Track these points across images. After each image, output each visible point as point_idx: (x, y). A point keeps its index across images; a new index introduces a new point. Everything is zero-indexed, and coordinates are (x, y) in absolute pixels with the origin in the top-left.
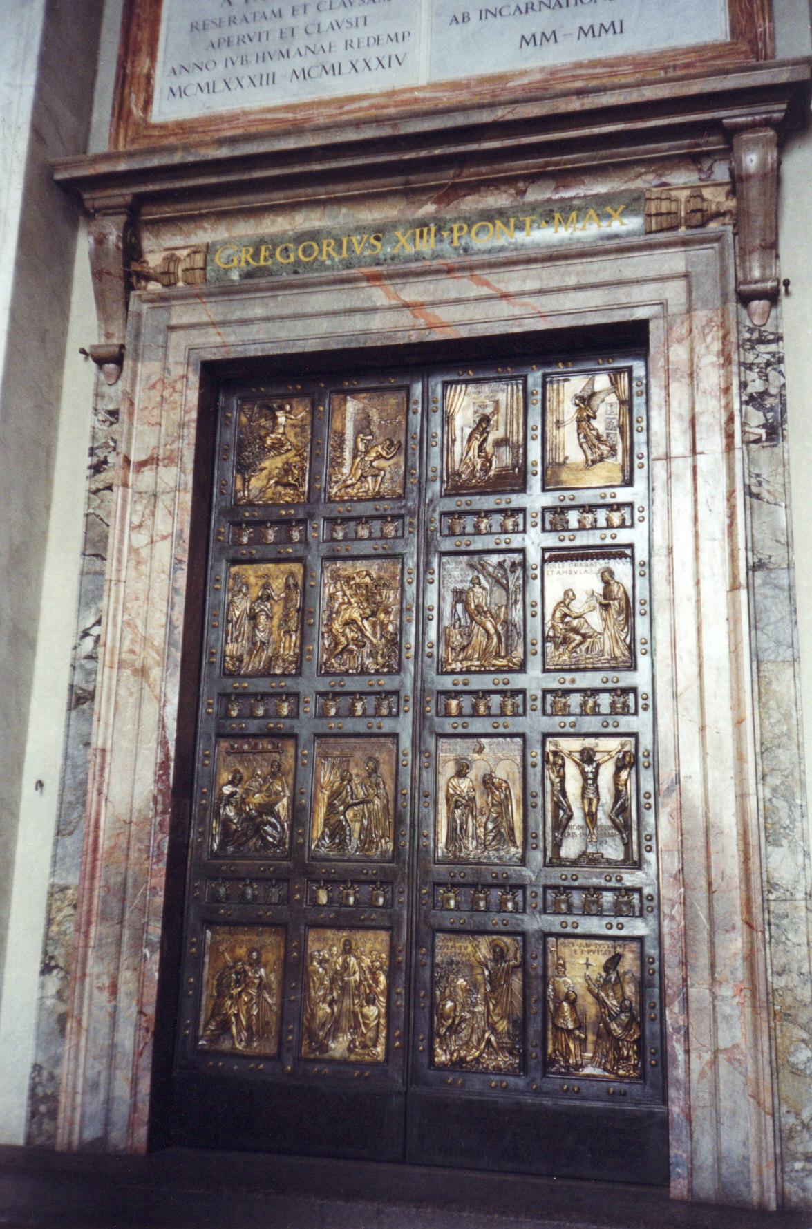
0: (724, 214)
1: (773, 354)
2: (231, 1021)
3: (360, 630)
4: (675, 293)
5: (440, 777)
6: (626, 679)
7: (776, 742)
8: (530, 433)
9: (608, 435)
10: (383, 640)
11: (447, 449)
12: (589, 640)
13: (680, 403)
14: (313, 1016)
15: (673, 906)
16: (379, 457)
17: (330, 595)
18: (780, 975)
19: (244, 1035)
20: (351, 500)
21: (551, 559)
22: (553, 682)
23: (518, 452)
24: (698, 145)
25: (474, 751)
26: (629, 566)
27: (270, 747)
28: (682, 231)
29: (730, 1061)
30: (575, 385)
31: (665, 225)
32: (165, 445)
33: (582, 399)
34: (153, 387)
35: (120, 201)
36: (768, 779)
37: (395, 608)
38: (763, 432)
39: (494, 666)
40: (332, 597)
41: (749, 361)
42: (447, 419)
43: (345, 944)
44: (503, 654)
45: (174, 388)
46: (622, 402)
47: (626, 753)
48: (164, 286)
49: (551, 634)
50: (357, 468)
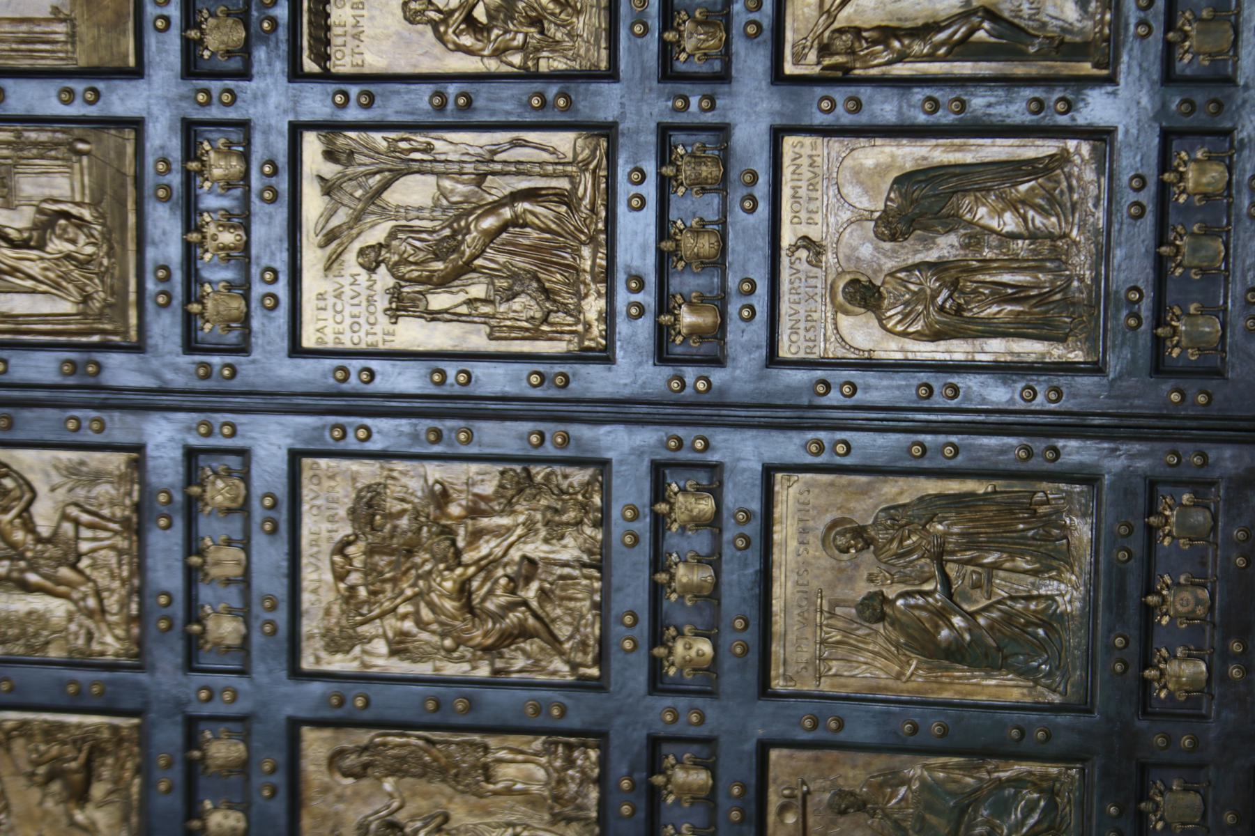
3: (487, 566)
5: (879, 355)
10: (518, 508)
17: (393, 653)
21: (322, 57)
23: (36, 144)
25: (815, 262)
27: (790, 819)
37: (434, 471)
39: (593, 210)
40: (400, 646)
44: (564, 184)
49: (517, 59)
50: (59, 582)
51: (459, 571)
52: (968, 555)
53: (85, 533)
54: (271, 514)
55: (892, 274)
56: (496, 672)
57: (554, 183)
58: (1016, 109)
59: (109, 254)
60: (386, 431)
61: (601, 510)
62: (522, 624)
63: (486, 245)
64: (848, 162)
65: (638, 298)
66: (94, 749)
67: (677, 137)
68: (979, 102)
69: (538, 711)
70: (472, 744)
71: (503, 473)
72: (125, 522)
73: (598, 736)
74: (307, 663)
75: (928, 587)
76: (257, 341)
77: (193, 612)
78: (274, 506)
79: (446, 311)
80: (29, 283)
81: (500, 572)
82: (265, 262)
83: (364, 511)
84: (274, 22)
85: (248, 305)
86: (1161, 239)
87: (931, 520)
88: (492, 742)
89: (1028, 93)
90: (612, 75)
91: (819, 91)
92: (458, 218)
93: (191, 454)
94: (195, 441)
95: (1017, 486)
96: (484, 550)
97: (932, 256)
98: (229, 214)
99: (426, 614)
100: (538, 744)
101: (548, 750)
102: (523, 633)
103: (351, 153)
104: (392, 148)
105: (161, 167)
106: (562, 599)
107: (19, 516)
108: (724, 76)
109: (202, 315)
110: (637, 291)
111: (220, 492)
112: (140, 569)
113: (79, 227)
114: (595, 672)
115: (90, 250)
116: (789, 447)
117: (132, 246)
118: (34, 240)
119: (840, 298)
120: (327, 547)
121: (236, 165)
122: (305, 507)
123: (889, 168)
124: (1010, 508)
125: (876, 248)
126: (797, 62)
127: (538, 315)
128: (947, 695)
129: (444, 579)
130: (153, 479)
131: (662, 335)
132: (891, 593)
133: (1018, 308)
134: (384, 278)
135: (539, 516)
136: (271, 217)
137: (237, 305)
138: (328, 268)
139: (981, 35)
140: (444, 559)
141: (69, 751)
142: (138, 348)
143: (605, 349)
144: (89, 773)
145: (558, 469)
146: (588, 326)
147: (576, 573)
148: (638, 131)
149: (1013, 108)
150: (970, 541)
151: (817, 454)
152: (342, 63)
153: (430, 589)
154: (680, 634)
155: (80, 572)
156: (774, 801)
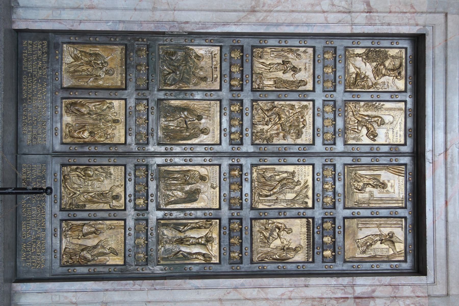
2: (79, 61)
3: (276, 124)
5: (200, 167)
6: (246, 259)
8: (375, 211)
10: (269, 135)
11: (369, 166)
12: (266, 241)
14: (83, 105)
15: (140, 285)
16: (368, 128)
17: (294, 106)
19: (72, 69)
20: (345, 116)
21: (308, 222)
22: (247, 223)
26: (303, 260)
30: (399, 233)
33: (391, 237)
34: (412, 7)
40: (293, 107)
42: (386, 166)
43: (118, 120)
44: (261, 198)
45: (411, 19)
46: (388, 257)
47: (211, 258)
49: (270, 222)
51: (281, 123)
52: (182, 129)
53: (356, 127)
54: (318, 133)
55: (198, 182)
56: (273, 103)
57: (263, 198)
58: (175, 214)
60: (295, 149)
61: (253, 135)
62: (268, 113)
63: (276, 186)
64: (206, 203)
65: (246, 177)
66: (355, 84)
67: (239, 207)
68: (182, 215)
69: (265, 95)
70: (278, 88)
71: (272, 142)
72: (348, 130)
74: (311, 103)
75: (189, 122)
76: (321, 167)
79: (284, 173)
80: (367, 177)
81: (273, 122)
82: (319, 182)
83: (300, 133)
84: (317, 228)
85: (323, 173)
86: (147, 190)
87: (189, 135)
88: (274, 89)
89: (173, 217)
90: (251, 219)
91: (212, 217)
92: (281, 191)
93: (335, 144)
94: (334, 146)
95: (173, 142)
96: (276, 127)
97: (190, 186)
98: (327, 191)
99: (287, 113)
100: (266, 89)
102: (268, 110)
104: (294, 204)
105: (340, 200)
106: (260, 117)
107: (369, 130)
108: (230, 219)
109: (332, 171)
110: (246, 178)
111: (329, 136)
113: (357, 188)
114: (254, 103)
115: (354, 183)
116: (217, 148)
117: (346, 184)
119: (207, 177)
120: (307, 126)
121: (325, 200)
122: (312, 134)
123: (199, 202)
124: (174, 138)
125: (200, 187)
126: (216, 222)
127: (265, 173)
128: (186, 101)
129: (284, 121)
131: (241, 170)
132: (196, 121)
133: (174, 176)
134: (296, 179)
135: (265, 133)
136: (318, 191)
137: (325, 173)
139: (182, 228)
140: (284, 125)
141: (359, 83)
142: (345, 165)
143: (252, 167)
144: (356, 79)
145: (261, 143)
146: (256, 171)
147: (258, 123)
148: (246, 209)
149: (176, 214)
150: (181, 131)
151: (211, 148)
152: (304, 220)
153: (286, 118)
154: (237, 112)
155: (357, 119)
156: (218, 79)
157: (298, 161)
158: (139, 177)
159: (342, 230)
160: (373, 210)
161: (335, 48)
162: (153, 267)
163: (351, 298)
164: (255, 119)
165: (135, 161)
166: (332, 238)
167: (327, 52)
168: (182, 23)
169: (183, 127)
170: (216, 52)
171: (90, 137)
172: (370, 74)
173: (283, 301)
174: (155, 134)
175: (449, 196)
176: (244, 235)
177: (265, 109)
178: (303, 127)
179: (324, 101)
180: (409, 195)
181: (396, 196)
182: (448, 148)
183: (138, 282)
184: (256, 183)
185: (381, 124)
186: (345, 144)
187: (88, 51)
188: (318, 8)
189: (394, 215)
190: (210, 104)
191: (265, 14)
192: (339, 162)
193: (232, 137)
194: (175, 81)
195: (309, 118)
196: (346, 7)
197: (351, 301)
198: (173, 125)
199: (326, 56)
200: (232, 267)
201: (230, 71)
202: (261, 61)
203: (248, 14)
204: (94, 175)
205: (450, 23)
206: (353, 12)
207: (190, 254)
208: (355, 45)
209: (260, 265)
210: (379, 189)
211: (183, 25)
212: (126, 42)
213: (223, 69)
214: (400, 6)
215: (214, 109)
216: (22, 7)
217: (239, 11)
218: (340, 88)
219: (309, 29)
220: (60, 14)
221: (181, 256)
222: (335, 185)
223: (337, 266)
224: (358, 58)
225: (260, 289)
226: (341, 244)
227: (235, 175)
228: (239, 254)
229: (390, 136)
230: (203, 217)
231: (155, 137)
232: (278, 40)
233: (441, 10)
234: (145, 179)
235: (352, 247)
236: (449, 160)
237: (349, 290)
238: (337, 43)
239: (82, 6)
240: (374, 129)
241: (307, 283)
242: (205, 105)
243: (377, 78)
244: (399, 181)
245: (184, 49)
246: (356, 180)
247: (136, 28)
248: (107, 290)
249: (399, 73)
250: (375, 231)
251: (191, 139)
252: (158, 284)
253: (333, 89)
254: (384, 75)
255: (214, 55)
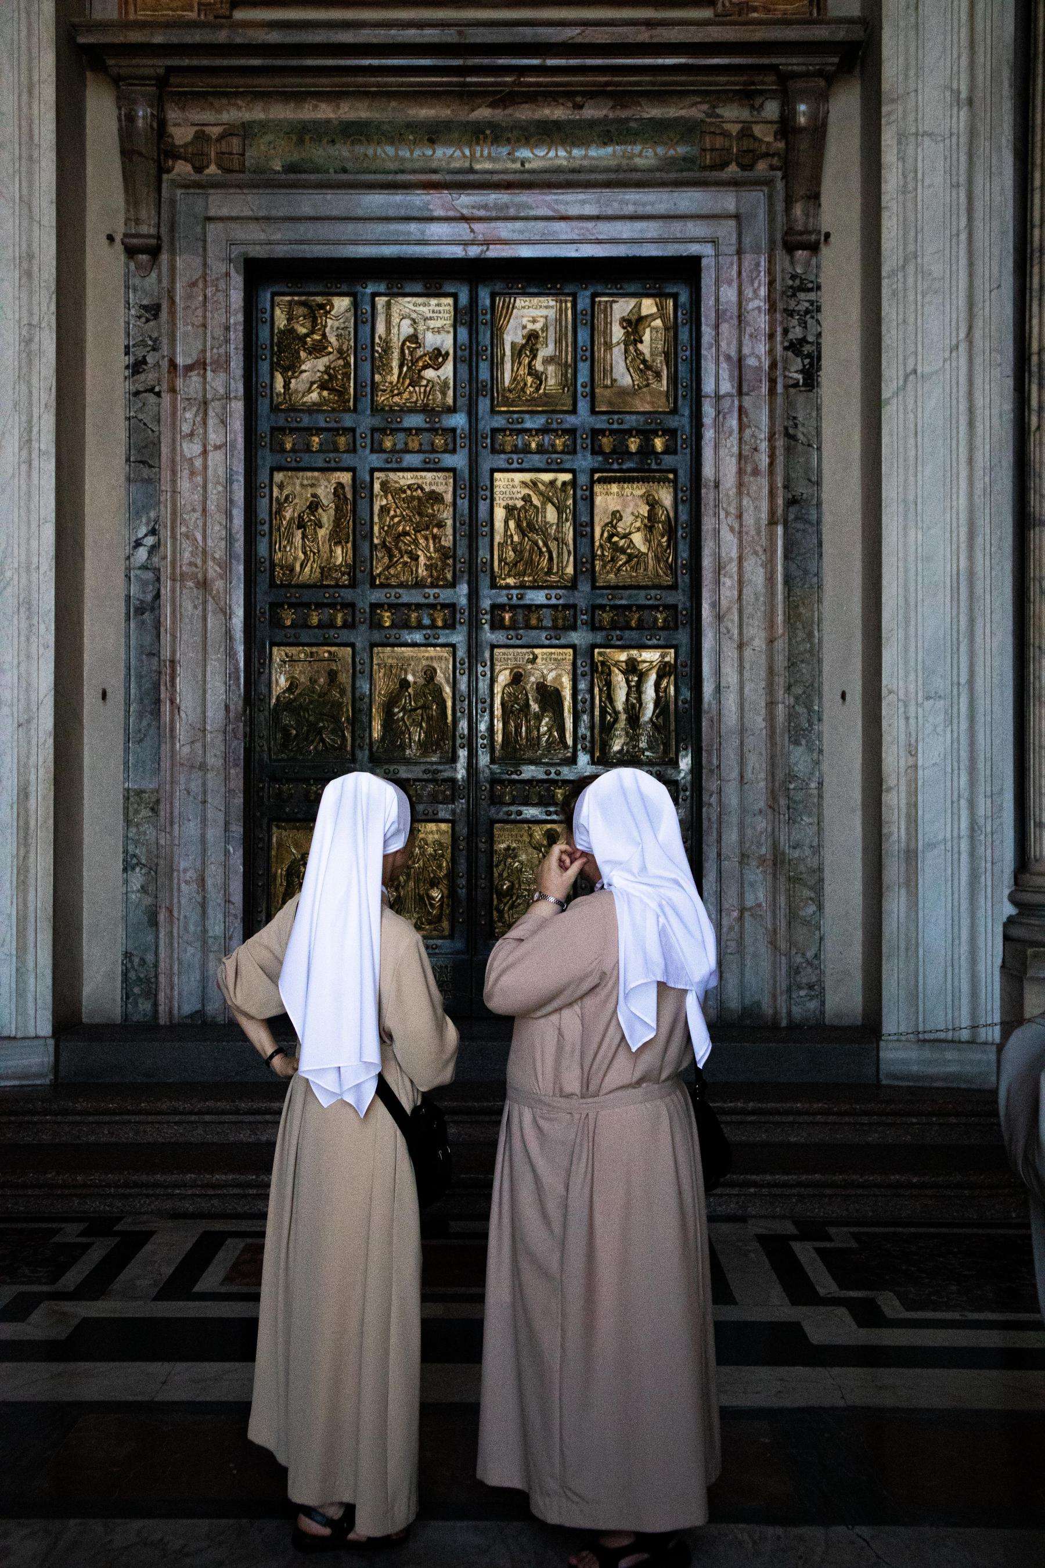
0: (773, 155)
1: (812, 303)
3: (415, 542)
4: (727, 230)
7: (801, 657)
9: (653, 361)
11: (496, 365)
13: (728, 344)
15: (711, 795)
16: (425, 367)
17: (382, 507)
18: (794, 848)
20: (401, 410)
21: (601, 481)
23: (566, 372)
24: (753, 83)
26: (671, 490)
28: (733, 168)
29: (752, 915)
30: (623, 307)
31: (718, 161)
32: (212, 349)
35: (151, 72)
36: (793, 689)
37: (449, 522)
38: (800, 377)
40: (384, 510)
41: (791, 308)
42: (497, 334)
44: (555, 570)
45: (216, 286)
46: (667, 329)
47: (666, 663)
48: (194, 167)
49: (599, 552)
50: (404, 379)
53: (422, 389)
55: (524, 688)
56: (376, 546)
57: (555, 567)
58: (583, 730)
59: (527, 400)
60: (464, 504)
65: (515, 598)
66: (342, 393)
69: (362, 562)
72: (427, 405)
73: (353, 584)
74: (376, 474)
76: (496, 457)
77: (394, 431)
78: (435, 463)
84: (612, 463)
88: (350, 545)
89: (588, 734)
90: (594, 587)
91: (589, 661)
93: (453, 430)
94: (458, 431)
95: (450, 734)
96: (421, 541)
97: (531, 703)
99: (396, 520)
100: (350, 561)
101: (347, 565)
102: (391, 557)
103: (565, 491)
104: (568, 507)
111: (439, 441)
112: (412, 411)
114: (378, 582)
116: (461, 653)
118: (532, 371)
120: (420, 482)
121: (560, 448)
123: (562, 687)
126: (600, 654)
130: (444, 416)
131: (501, 607)
132: (410, 690)
134: (520, 504)
137: (509, 448)
138: (523, 482)
141: (340, 383)
142: (493, 411)
144: (331, 390)
146: (504, 579)
150: (430, 718)
152: (597, 488)
154: (392, 614)
156: (333, 649)
157: (485, 500)
158: (514, 796)
159: (616, 417)
160: (579, 357)
161: (273, 429)
162: (680, 772)
163: (740, 401)
164: (407, 581)
165: (484, 804)
166: (631, 436)
167: (282, 444)
168: (227, 717)
169: (422, 715)
170: (283, 653)
171: (440, 886)
172: (321, 363)
173: (744, 529)
174: (435, 767)
175: (550, 213)
176: (624, 602)
177: (386, 560)
178: (422, 489)
179: (372, 451)
180: (549, 289)
181: (552, 313)
182: (458, 215)
183: (705, 798)
184: (526, 579)
185: (417, 343)
186: (453, 410)
187: (282, 889)
188: (198, 463)
189: (589, 318)
190: (378, 664)
191: (210, 563)
192: (488, 423)
193: (440, 623)
194: (338, 730)
195: (406, 479)
196: (195, 409)
197: (747, 402)
198: (417, 735)
199: (288, 446)
200: (682, 623)
201: (318, 627)
202: (298, 568)
203: (210, 594)
204: (512, 878)
205: (225, 212)
206: (204, 396)
207: (657, 702)
208: (268, 392)
209: (679, 572)
210: (539, 346)
211: (232, 715)
212: (266, 820)
213: (313, 641)
214: (193, 307)
215: (389, 657)
216: (203, 1005)
217: (205, 610)
218: (348, 421)
219: (237, 481)
220: (215, 938)
221: (661, 720)
222: (529, 430)
223: (683, 426)
224: (292, 386)
225: (722, 572)
226: (642, 419)
227: (511, 618)
228: (658, 610)
229: (439, 324)
230: (588, 678)
231: (440, 767)
232: (259, 537)
233: (199, 229)
234: (519, 786)
235: (648, 398)
236: (482, 213)
237: (726, 404)
238: (264, 426)
239: (199, 899)
240: (425, 355)
241: (712, 484)
242: (381, 674)
243: (330, 349)
244: (524, 307)
245: (277, 714)
246: (523, 390)
247: (239, 800)
248: (719, 855)
249: (322, 306)
250: (618, 352)
251: (444, 702)
252: (710, 762)
253: (351, 434)
254: (324, 336)
255: (287, 656)
